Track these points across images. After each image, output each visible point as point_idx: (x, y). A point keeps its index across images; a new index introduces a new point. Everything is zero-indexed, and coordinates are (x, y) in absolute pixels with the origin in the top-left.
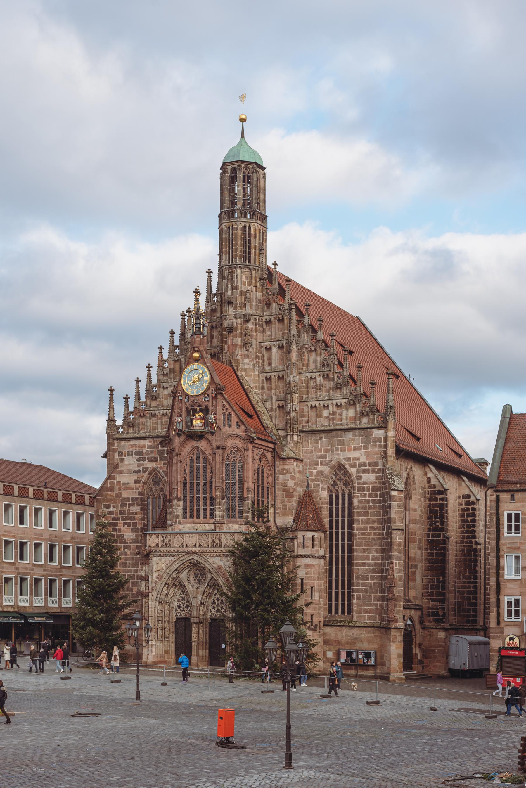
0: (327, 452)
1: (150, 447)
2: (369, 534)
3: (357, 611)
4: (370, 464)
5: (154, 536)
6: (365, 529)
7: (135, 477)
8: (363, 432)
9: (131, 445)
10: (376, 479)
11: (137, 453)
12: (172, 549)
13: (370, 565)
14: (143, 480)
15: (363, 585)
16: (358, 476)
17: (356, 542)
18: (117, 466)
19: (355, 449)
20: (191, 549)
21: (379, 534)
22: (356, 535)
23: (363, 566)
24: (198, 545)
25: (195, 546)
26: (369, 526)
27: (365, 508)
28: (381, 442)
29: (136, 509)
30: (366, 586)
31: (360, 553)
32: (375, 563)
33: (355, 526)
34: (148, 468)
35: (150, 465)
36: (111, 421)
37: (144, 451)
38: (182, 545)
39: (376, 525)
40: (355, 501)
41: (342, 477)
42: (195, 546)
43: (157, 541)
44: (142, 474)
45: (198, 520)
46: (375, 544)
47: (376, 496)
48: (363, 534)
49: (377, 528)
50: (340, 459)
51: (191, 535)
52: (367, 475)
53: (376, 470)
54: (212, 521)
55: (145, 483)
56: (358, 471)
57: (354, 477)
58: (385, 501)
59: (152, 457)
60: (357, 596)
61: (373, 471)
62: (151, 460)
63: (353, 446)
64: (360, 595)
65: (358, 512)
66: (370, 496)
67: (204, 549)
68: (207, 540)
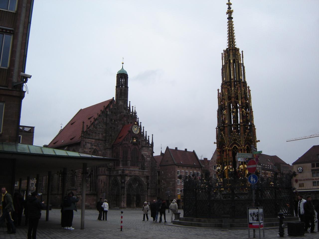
1: (95, 142)
5: (127, 171)
7: (90, 150)
9: (89, 141)
11: (91, 143)
12: (132, 174)
14: (92, 151)
19: (146, 151)
34: (93, 148)
35: (94, 147)
37: (93, 143)
38: (134, 174)
40: (146, 164)
43: (128, 172)
44: (92, 150)
45: (134, 167)
54: (138, 167)
56: (146, 157)
57: (145, 158)
61: (150, 158)
62: (95, 146)
67: (140, 175)
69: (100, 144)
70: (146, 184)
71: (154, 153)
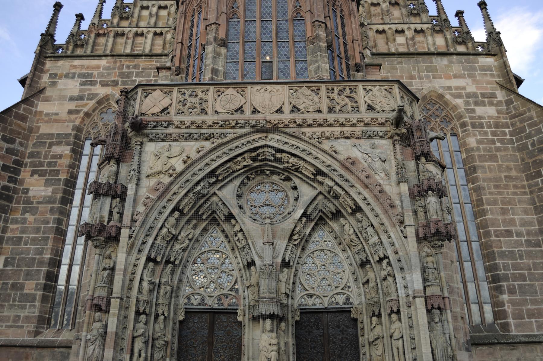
0: (412, 79)
1: (108, 68)
2: (506, 187)
3: (513, 314)
4: (483, 95)
6: (496, 179)
7: (72, 106)
8: (463, 58)
9: (75, 67)
10: (498, 113)
12: (210, 118)
13: (519, 234)
14: (85, 110)
15: (516, 267)
16: (468, 109)
17: (487, 199)
18: (42, 91)
19: (455, 77)
20: (269, 117)
21: (524, 187)
22: (484, 189)
23: (509, 236)
24: (287, 109)
25: (280, 111)
26: (503, 175)
27: (490, 150)
28: (492, 71)
29: (66, 150)
30: (521, 269)
31: (498, 215)
32: (528, 230)
33: (480, 174)
34: (97, 95)
36: (48, 37)
37: (95, 73)
38: (240, 110)
39: (514, 173)
41: (437, 113)
42: (282, 112)
43: (166, 102)
46: (520, 201)
47: (505, 134)
48: (496, 187)
49: (517, 178)
50: (434, 87)
51: (268, 87)
52: (483, 108)
53: (495, 102)
55: (87, 115)
56: (467, 103)
58: (529, 136)
59: (109, 81)
60: (508, 286)
61: (491, 104)
62: (104, 84)
63: (452, 73)
64: (514, 285)
65: (480, 156)
66: (494, 134)
67: (310, 117)
68: (316, 98)
69: (137, 75)
70: (404, 188)
71: (519, 81)
